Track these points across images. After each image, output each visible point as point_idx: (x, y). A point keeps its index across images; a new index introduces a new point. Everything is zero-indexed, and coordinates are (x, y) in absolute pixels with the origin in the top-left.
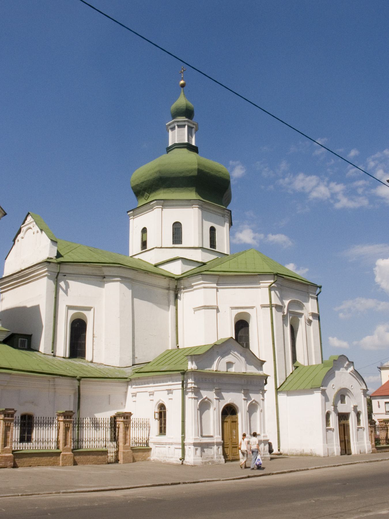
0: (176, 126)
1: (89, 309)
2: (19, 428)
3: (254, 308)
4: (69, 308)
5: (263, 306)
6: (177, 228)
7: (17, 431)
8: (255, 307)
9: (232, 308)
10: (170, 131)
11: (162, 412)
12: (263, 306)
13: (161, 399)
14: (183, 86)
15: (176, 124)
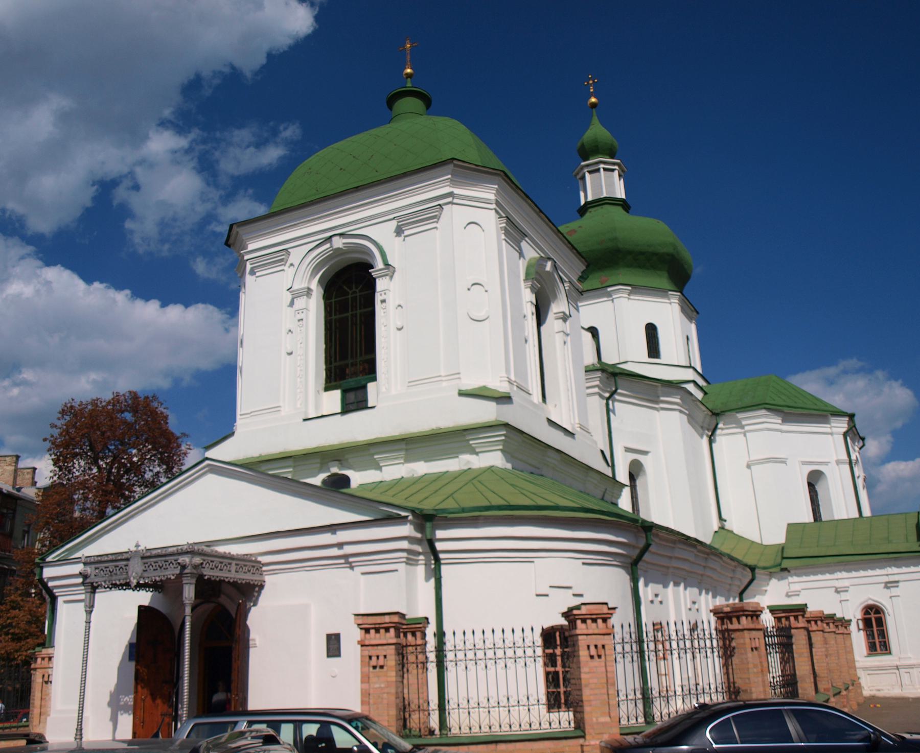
0: (602, 170)
1: (645, 453)
2: (635, 658)
3: (829, 464)
4: (628, 450)
5: (838, 462)
6: (651, 330)
7: (629, 666)
8: (829, 462)
9: (805, 463)
10: (588, 177)
11: (870, 619)
12: (838, 462)
13: (871, 597)
14: (594, 105)
15: (602, 166)
